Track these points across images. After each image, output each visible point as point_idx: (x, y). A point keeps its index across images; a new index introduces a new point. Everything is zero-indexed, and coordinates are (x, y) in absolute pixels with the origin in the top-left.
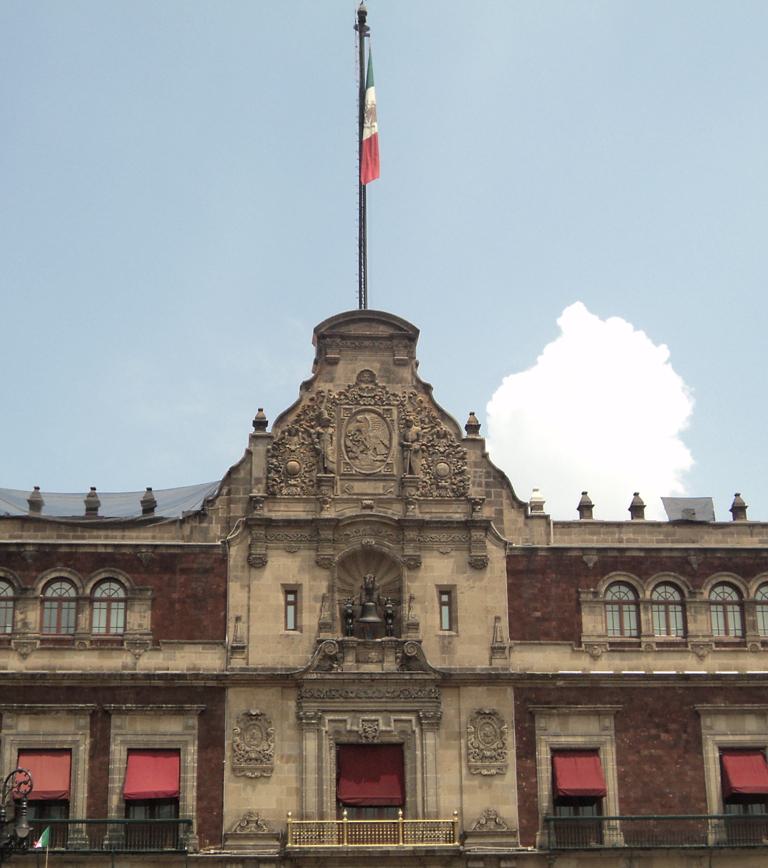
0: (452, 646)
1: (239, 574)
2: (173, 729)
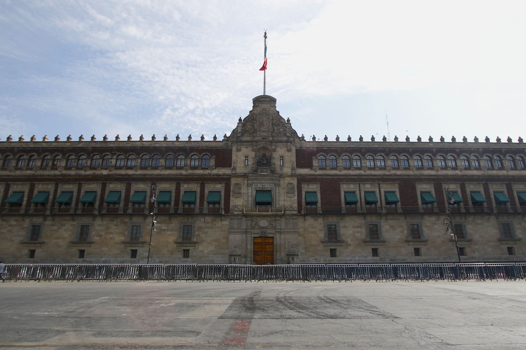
2: (219, 187)
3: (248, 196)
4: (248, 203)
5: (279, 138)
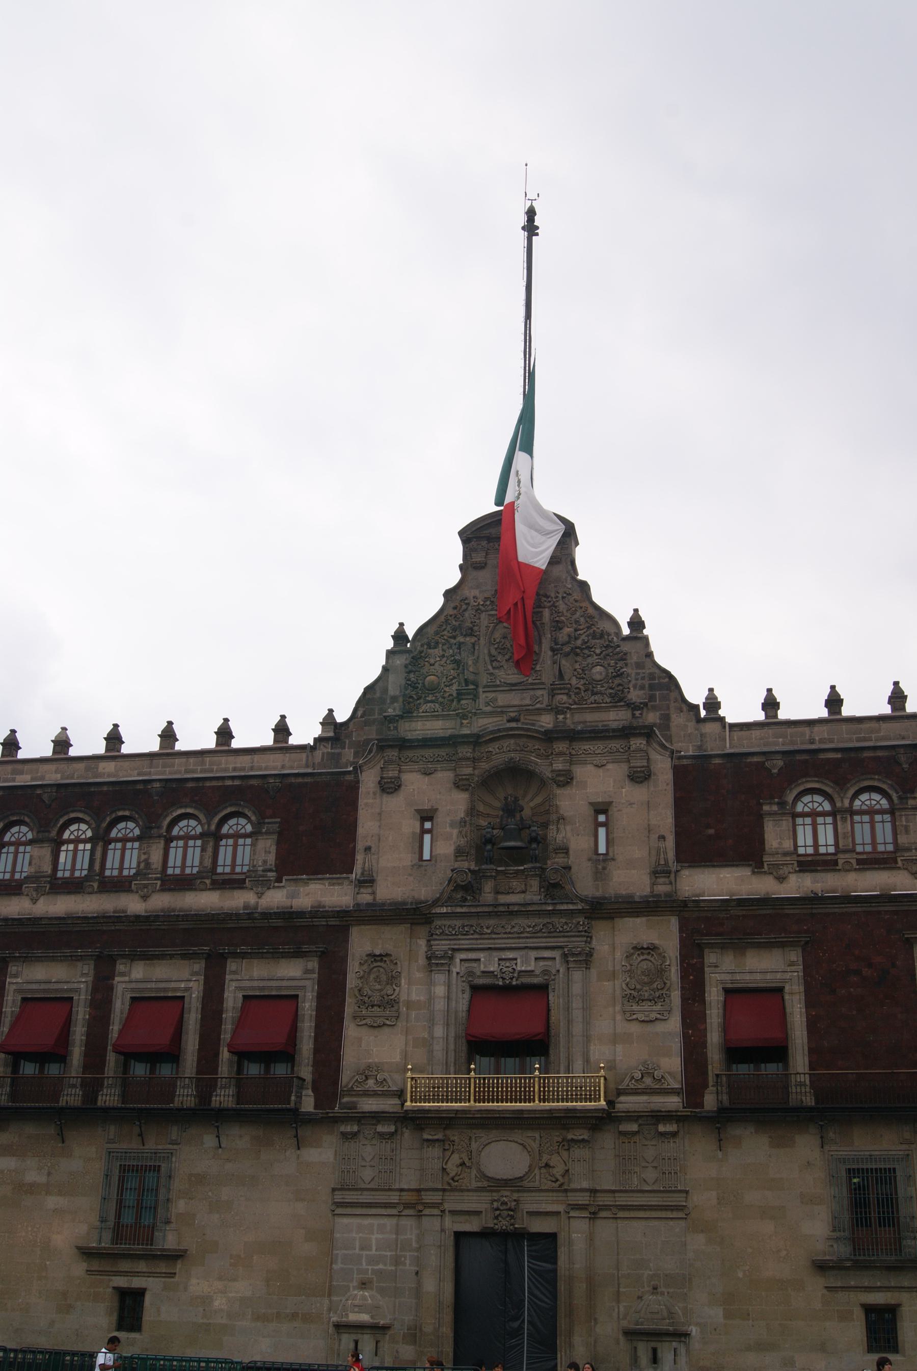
0: (606, 872)
1: (371, 801)
2: (293, 974)
3: (432, 1021)
4: (431, 1052)
5: (590, 717)
